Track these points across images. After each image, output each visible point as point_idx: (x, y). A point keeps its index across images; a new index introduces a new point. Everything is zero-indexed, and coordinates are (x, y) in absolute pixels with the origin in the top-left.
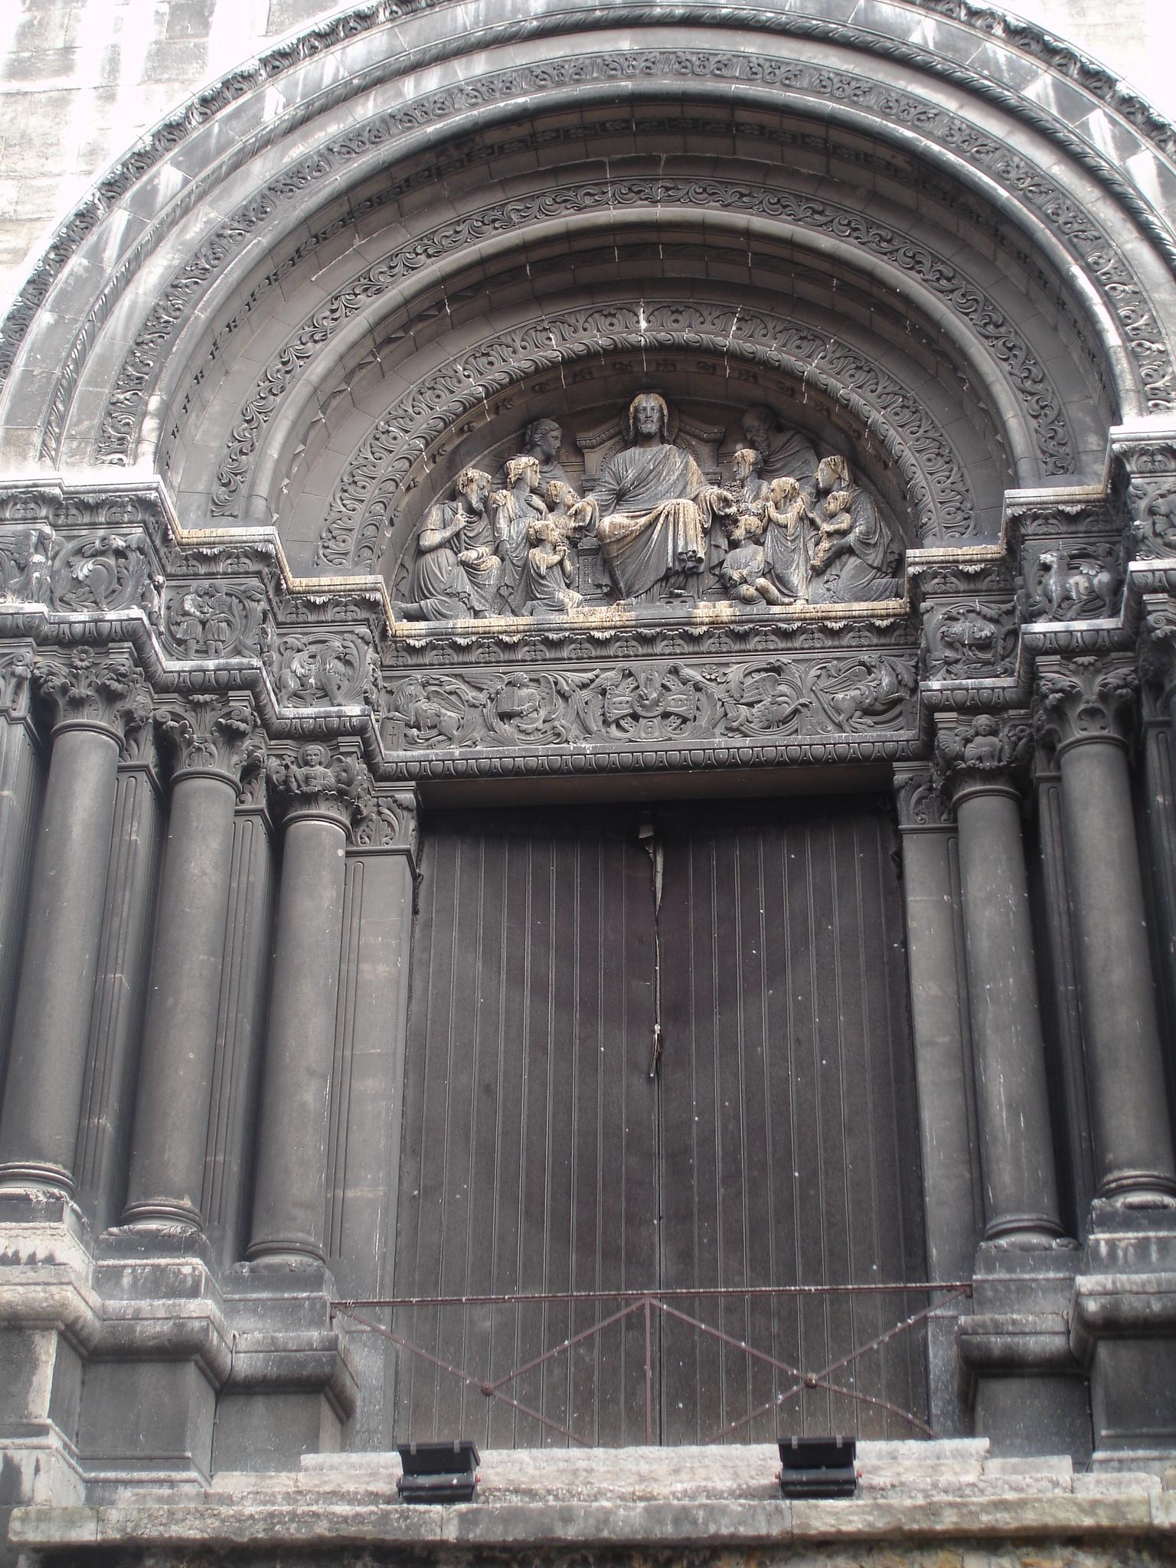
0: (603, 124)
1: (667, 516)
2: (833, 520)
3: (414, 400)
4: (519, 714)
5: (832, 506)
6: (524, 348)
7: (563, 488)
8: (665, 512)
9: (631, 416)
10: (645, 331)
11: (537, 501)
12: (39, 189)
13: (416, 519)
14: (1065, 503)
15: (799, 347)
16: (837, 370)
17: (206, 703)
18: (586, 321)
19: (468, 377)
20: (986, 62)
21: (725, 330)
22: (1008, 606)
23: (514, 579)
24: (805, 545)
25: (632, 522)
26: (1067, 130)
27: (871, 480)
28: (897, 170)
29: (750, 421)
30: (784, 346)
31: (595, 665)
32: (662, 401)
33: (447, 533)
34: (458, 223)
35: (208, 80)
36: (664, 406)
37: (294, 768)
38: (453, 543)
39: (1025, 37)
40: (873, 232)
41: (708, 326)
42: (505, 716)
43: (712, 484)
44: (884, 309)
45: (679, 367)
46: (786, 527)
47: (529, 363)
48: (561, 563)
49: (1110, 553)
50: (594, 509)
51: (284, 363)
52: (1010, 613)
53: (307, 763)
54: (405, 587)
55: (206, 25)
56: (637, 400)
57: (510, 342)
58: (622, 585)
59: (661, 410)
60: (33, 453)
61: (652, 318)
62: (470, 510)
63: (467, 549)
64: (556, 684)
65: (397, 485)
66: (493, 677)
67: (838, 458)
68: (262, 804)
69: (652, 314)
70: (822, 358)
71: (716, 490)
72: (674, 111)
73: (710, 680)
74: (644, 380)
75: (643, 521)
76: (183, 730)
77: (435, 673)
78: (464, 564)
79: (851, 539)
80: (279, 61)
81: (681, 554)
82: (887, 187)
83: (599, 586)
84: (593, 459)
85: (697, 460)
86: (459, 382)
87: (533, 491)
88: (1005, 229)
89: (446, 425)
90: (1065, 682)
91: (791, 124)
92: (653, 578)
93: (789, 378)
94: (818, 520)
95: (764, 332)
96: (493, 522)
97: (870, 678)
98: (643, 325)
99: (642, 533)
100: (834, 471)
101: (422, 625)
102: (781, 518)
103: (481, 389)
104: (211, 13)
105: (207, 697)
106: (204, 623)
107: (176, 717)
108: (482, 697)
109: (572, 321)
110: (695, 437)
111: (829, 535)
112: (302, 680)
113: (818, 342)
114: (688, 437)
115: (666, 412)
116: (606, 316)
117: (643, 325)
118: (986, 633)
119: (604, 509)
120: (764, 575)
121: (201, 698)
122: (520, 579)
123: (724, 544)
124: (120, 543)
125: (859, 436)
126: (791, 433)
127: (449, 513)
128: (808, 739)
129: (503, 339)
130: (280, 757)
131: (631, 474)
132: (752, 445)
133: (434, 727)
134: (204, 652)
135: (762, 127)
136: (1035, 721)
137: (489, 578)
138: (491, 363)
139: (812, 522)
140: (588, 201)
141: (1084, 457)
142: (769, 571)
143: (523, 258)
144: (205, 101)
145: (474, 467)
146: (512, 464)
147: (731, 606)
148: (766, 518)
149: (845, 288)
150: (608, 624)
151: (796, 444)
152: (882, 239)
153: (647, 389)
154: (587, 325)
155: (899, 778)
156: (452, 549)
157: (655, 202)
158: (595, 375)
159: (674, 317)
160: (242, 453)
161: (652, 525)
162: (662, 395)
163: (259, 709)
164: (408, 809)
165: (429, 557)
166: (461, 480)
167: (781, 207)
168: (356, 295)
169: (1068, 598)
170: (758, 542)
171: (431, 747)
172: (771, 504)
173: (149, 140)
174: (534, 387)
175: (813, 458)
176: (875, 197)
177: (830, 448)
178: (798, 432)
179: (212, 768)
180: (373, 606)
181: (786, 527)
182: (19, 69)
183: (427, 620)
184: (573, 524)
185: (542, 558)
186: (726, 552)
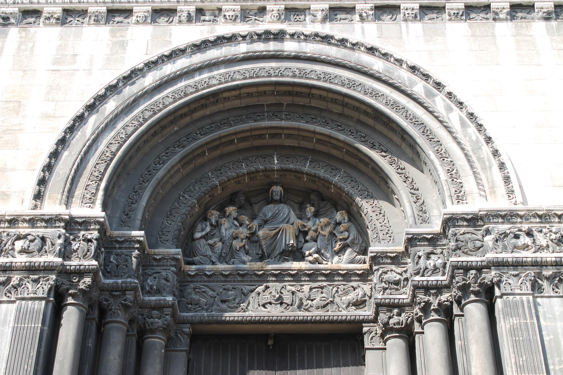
0: (265, 92)
1: (283, 230)
2: (342, 234)
3: (193, 185)
4: (228, 301)
5: (341, 228)
6: (233, 168)
7: (245, 219)
8: (282, 229)
9: (270, 193)
10: (277, 164)
11: (236, 223)
13: (192, 229)
14: (426, 234)
15: (331, 172)
16: (344, 181)
17: (118, 295)
18: (256, 159)
19: (213, 177)
20: (399, 77)
21: (305, 165)
22: (405, 269)
23: (227, 251)
24: (331, 242)
25: (271, 232)
26: (428, 102)
27: (355, 219)
28: (368, 113)
29: (313, 197)
30: (326, 171)
31: (256, 284)
32: (281, 189)
33: (204, 233)
34: (212, 123)
35: (125, 70)
36: (282, 190)
37: (147, 319)
38: (206, 237)
39: (413, 69)
40: (359, 134)
41: (298, 163)
42: (223, 301)
43: (298, 218)
44: (361, 160)
45: (288, 177)
46: (325, 236)
47: (235, 174)
48: (244, 246)
49: (442, 253)
50: (256, 226)
51: (149, 171)
52: (406, 272)
53: (152, 318)
54: (187, 252)
55: (124, 49)
56: (272, 188)
57: (228, 166)
58: (266, 254)
59: (281, 191)
60: (58, 202)
61: (279, 159)
62: (211, 225)
63: (210, 239)
64: (242, 290)
65: (187, 216)
66: (219, 287)
67: (344, 212)
68: (135, 332)
69: (279, 158)
70: (339, 176)
71: (300, 221)
72: (290, 89)
73: (297, 291)
74: (275, 180)
75: (274, 232)
76: (109, 305)
77: (198, 284)
78: (209, 245)
79: (348, 241)
80: (151, 65)
81: (288, 244)
82: (364, 118)
83: (258, 254)
84: (256, 207)
85: (293, 210)
86: (210, 179)
87: (235, 219)
88: (405, 136)
89: (205, 195)
90: (426, 298)
91: (331, 95)
92: (278, 252)
93: (327, 183)
94: (337, 234)
95: (319, 166)
96: (220, 230)
97: (355, 292)
98: (276, 162)
99: (274, 236)
100: (342, 216)
101: (194, 267)
102: (323, 233)
103: (217, 182)
104: (127, 45)
105: (118, 293)
106: (117, 266)
107: (106, 300)
108: (215, 294)
109: (250, 159)
110: (292, 201)
111: (341, 240)
112: (151, 287)
113: (338, 171)
114: (290, 201)
115: (282, 192)
116: (263, 158)
117: (276, 162)
118: (397, 278)
119: (260, 226)
120: (317, 253)
121: (116, 293)
122: (229, 251)
123: (303, 241)
124: (89, 237)
125: (352, 204)
126: (326, 202)
127: (204, 226)
128: (332, 314)
129: (226, 165)
130: (142, 315)
131: (270, 214)
132: (313, 205)
133: (197, 304)
134: (117, 276)
135: (321, 96)
136: (414, 312)
137: (218, 250)
138: (221, 173)
139: (334, 234)
140: (258, 118)
141: (432, 218)
142: (318, 252)
143: (234, 137)
144: (124, 78)
145: (213, 209)
146: (227, 209)
147: (305, 264)
148: (318, 233)
149: (348, 152)
150: (261, 269)
151: (329, 206)
152: (362, 137)
153: (276, 184)
154: (256, 161)
155: (365, 329)
156: (205, 239)
157: (282, 120)
158: (258, 178)
159: (287, 159)
160: (132, 203)
161: (278, 233)
162: (282, 186)
163: (136, 297)
164: (187, 335)
165: (197, 241)
166: (209, 214)
167: (326, 124)
168: (175, 148)
169: (426, 268)
170: (316, 241)
171: (196, 312)
172: (319, 227)
173: (103, 91)
174: (236, 182)
175: (335, 212)
176: (359, 122)
177: (340, 207)
178: (330, 201)
179: (118, 319)
180: (177, 260)
181: (325, 236)
182: (57, 61)
183: (195, 264)
184: (249, 232)
185: (237, 244)
186: (304, 244)
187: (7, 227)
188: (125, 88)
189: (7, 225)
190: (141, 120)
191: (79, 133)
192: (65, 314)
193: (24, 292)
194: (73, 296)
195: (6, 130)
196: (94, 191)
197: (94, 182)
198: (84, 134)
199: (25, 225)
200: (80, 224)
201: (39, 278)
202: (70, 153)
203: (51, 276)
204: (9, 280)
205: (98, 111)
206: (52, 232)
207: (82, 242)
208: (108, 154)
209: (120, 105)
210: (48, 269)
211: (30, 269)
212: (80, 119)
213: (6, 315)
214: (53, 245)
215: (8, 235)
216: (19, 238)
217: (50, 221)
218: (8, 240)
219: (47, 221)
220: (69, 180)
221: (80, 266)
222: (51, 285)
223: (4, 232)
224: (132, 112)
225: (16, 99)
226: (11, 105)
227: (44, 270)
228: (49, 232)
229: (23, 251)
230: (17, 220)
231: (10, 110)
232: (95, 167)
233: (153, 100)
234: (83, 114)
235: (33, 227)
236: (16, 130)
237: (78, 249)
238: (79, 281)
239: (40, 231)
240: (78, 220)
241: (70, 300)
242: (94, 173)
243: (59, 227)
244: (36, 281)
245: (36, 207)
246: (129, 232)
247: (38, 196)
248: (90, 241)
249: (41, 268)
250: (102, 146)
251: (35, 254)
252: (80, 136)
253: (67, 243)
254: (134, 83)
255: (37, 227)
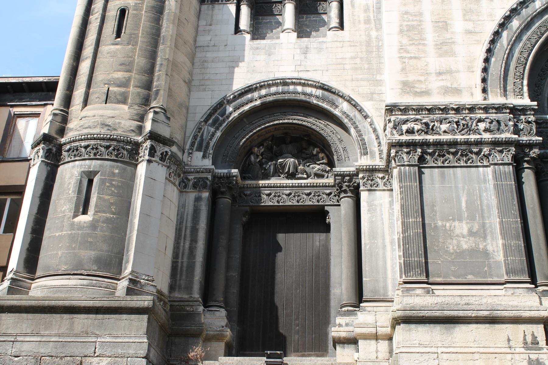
12: (479, 24)
60: (499, 95)
173: (509, 13)
187: (468, 113)
188: (522, 10)
189: (467, 111)
190: (539, 33)
191: (498, 44)
192: (523, 175)
193: (494, 159)
194: (528, 162)
195: (443, 43)
196: (521, 87)
197: (518, 80)
198: (502, 45)
199: (481, 111)
200: (520, 110)
201: (503, 149)
202: (496, 59)
203: (511, 148)
204: (480, 151)
205: (507, 28)
206: (502, 117)
207: (524, 123)
208: (522, 60)
209: (523, 23)
210: (508, 143)
211: (495, 143)
212: (497, 34)
213: (484, 176)
214: (506, 126)
215: (471, 119)
216: (480, 120)
217: (499, 109)
218: (472, 122)
219: (496, 109)
220: (502, 79)
221: (530, 140)
222: (513, 154)
223: (466, 116)
224: (531, 28)
225: (442, 20)
226: (440, 24)
227: (505, 144)
228: (500, 116)
229: (486, 130)
230: (475, 108)
231: (441, 28)
232: (516, 69)
233: (544, 19)
234: (498, 31)
235: (487, 113)
236: (450, 43)
237: (523, 129)
238: (529, 152)
239: (493, 116)
240: (518, 108)
241: (526, 165)
242: (517, 74)
243: (506, 113)
244: (501, 152)
245: (485, 99)
246: (545, 116)
247: (484, 91)
248: (529, 122)
249: (503, 143)
250: (516, 54)
251: (495, 132)
252: (499, 46)
253: (515, 125)
254: (527, 7)
255: (490, 113)
